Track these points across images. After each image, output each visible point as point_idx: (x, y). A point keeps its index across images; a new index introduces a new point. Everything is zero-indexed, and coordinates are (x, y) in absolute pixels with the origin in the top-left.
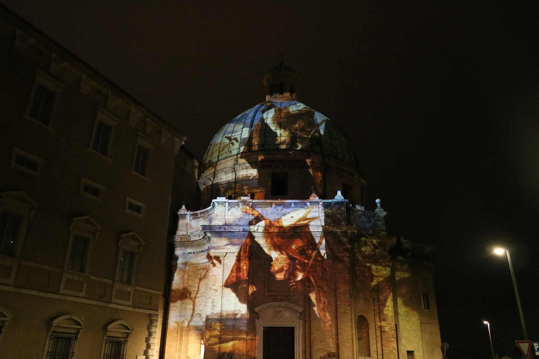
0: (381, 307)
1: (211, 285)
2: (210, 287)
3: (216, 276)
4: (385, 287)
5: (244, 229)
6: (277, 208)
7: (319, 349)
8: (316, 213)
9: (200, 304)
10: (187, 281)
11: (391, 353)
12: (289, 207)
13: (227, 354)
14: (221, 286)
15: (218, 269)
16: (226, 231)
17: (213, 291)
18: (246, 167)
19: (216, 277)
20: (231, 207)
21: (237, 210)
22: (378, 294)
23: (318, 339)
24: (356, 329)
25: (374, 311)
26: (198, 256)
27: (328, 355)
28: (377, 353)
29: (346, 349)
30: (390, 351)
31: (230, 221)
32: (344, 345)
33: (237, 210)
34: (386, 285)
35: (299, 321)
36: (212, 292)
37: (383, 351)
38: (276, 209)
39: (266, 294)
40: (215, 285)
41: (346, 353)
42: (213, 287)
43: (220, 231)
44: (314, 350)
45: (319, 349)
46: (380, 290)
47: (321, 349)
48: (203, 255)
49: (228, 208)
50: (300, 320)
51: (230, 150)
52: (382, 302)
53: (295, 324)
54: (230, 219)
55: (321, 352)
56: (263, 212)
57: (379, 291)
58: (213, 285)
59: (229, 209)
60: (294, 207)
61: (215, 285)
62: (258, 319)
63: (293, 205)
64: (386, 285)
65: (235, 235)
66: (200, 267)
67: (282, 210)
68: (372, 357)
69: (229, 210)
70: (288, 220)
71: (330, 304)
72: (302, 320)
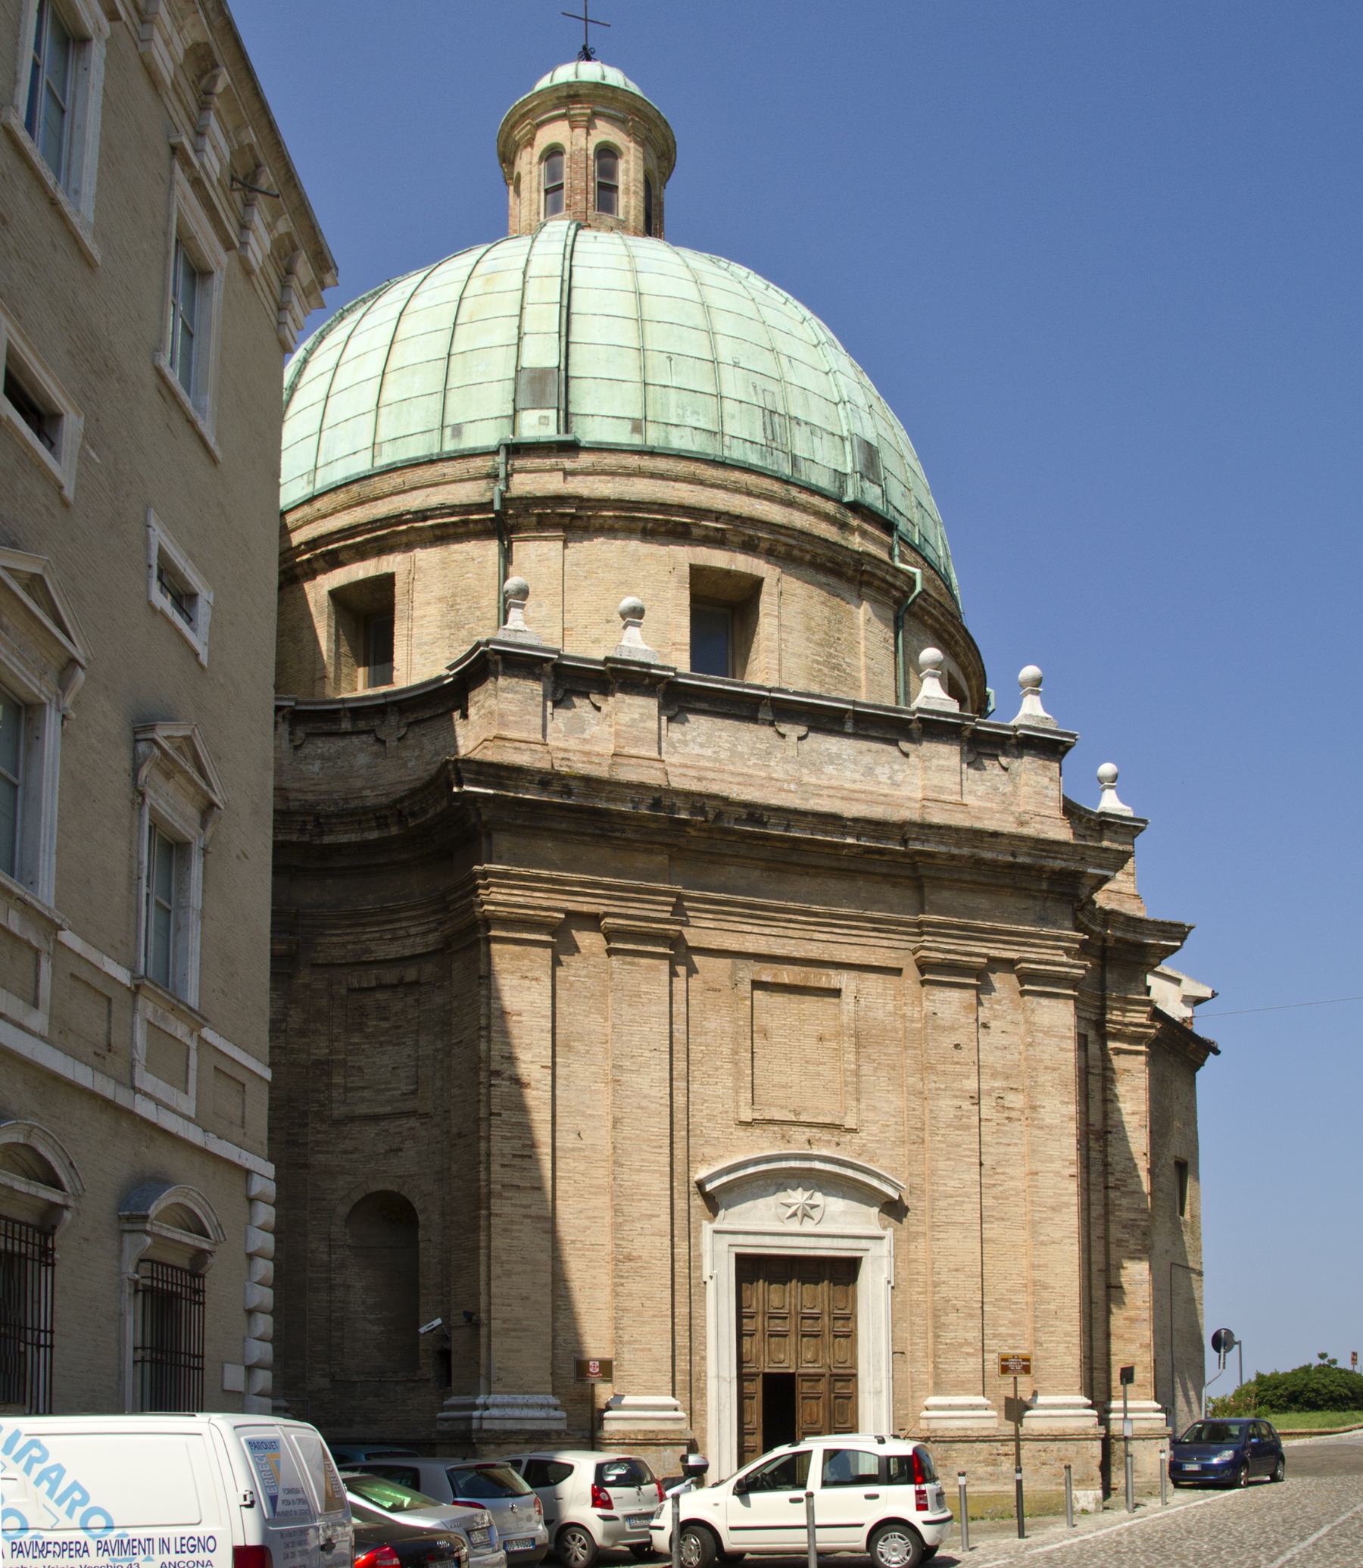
1: (498, 1058)
2: (495, 1066)
3: (519, 1015)
6: (781, 730)
7: (961, 1345)
8: (946, 776)
9: (391, 1150)
13: (597, 1363)
15: (527, 983)
17: (506, 1086)
19: (520, 1022)
21: (598, 709)
22: (1106, 1146)
26: (364, 925)
27: (1003, 1366)
29: (1058, 1342)
31: (568, 759)
32: (1051, 1329)
36: (507, 1090)
39: (747, 1115)
41: (1056, 1357)
45: (961, 1345)
48: (399, 920)
50: (885, 1228)
51: (451, 420)
53: (864, 1244)
54: (566, 750)
56: (720, 737)
63: (849, 728)
65: (607, 826)
66: (377, 979)
67: (800, 739)
70: (832, 792)
71: (999, 1170)
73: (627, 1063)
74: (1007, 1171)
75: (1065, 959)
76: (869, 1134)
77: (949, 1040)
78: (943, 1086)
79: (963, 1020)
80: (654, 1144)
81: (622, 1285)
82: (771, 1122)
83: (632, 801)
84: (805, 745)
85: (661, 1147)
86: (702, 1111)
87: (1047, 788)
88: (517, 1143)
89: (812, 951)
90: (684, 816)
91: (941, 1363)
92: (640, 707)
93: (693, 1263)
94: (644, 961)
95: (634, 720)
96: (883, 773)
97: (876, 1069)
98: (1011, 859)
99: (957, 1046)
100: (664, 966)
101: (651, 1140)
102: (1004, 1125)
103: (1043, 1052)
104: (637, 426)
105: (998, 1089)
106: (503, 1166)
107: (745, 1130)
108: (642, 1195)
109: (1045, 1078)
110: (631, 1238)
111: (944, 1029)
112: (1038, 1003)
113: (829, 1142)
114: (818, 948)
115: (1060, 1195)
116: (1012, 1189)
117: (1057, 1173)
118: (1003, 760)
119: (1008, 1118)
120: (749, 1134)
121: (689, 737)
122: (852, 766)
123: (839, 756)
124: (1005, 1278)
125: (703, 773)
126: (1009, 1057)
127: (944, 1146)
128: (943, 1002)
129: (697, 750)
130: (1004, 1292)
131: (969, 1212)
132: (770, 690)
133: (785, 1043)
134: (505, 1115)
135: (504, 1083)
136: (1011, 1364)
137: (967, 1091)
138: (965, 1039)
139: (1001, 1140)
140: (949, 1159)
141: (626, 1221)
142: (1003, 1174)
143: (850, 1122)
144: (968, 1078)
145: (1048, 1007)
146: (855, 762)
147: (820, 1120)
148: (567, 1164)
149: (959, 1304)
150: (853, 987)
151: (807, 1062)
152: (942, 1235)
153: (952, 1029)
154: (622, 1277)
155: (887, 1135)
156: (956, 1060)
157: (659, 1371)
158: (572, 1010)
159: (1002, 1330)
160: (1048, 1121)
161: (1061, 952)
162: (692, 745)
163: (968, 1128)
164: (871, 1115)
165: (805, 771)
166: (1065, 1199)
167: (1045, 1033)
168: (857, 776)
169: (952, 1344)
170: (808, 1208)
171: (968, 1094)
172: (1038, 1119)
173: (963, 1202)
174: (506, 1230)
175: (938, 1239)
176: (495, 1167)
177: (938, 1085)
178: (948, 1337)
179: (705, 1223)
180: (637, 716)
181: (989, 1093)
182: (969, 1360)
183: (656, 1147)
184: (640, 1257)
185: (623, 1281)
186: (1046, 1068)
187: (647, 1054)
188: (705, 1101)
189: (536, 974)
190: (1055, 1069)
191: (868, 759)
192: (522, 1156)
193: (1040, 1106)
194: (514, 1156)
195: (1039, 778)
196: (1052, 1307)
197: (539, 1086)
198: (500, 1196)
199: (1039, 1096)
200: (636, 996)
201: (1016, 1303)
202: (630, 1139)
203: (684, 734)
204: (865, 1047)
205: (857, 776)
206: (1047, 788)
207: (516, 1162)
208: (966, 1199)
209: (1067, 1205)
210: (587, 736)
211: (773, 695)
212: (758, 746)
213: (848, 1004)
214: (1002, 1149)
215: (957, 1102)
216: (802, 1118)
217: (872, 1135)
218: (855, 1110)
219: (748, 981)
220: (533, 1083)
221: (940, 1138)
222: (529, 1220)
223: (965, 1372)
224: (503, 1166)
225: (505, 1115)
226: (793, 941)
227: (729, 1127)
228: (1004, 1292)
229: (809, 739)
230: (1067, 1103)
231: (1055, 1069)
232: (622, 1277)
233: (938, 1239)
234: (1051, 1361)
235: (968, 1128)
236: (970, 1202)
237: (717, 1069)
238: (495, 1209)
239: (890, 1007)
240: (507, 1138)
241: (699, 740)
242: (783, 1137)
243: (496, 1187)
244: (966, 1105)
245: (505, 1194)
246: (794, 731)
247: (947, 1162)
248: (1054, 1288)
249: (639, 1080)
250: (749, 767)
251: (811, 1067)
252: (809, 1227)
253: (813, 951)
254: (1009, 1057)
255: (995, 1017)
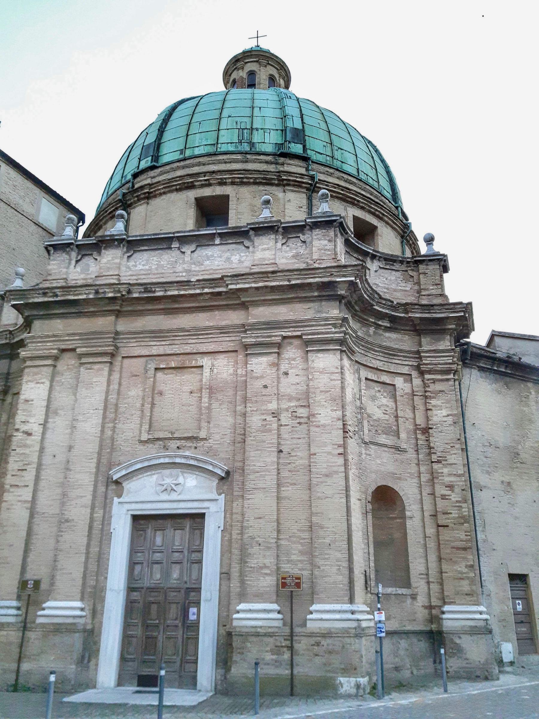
0: (435, 466)
2: (17, 427)
3: (32, 401)
4: (445, 419)
5: (97, 292)
6: (183, 250)
7: (261, 568)
10: (5, 427)
11: (462, 579)
12: (208, 245)
14: (41, 424)
15: (38, 385)
16: (59, 299)
17: (21, 436)
18: (145, 193)
19: (31, 404)
20: (84, 256)
21: (96, 259)
23: (260, 542)
24: (370, 516)
25: (419, 477)
27: (282, 582)
28: (428, 578)
30: (462, 573)
32: (326, 556)
33: (96, 259)
34: (448, 416)
35: (217, 497)
36: (21, 438)
37: (443, 574)
38: (181, 252)
39: (145, 437)
40: (28, 422)
41: (330, 576)
42: (22, 426)
43: (46, 299)
44: (250, 569)
45: (261, 568)
46: (432, 428)
47: (266, 567)
49: (77, 258)
50: (220, 494)
52: (439, 454)
53: (206, 504)
55: (266, 574)
56: (153, 260)
57: (430, 430)
58: (24, 422)
59: (79, 258)
60: (221, 244)
61: (28, 422)
62: (119, 496)
64: (448, 416)
68: (416, 588)
69: (77, 261)
71: (292, 454)
72: (223, 495)
73: (80, 418)
74: (298, 454)
75: (333, 330)
76: (214, 441)
77: (259, 384)
78: (255, 409)
79: (268, 372)
80: (90, 457)
81: (62, 536)
82: (158, 439)
83: (86, 294)
84: (195, 255)
85: (92, 459)
86: (122, 438)
87: (326, 245)
88: (21, 464)
89: (187, 349)
90: (111, 295)
91: (247, 580)
92: (112, 254)
93: (106, 520)
94: (96, 367)
95: (109, 260)
96: (235, 258)
97: (220, 404)
98: (288, 283)
99: (265, 387)
100: (106, 368)
101: (87, 456)
102: (296, 427)
103: (319, 382)
104: (182, 152)
105: (293, 407)
106: (13, 475)
107: (144, 445)
108: (79, 485)
109: (320, 397)
110: (70, 509)
111: (257, 378)
112: (316, 356)
113: (190, 447)
114: (191, 347)
115: (331, 466)
116: (302, 465)
117: (329, 453)
118: (302, 237)
119: (299, 423)
120: (145, 447)
121: (138, 263)
122: (219, 259)
123: (212, 256)
124: (296, 522)
125: (140, 277)
126: (301, 388)
127: (254, 442)
128: (256, 364)
129: (141, 267)
130: (296, 531)
131: (270, 481)
132: (174, 233)
133: (172, 397)
134: (18, 450)
135: (20, 434)
136: (288, 581)
137: (271, 410)
138: (270, 382)
139: (294, 436)
140: (257, 450)
141: (68, 500)
142: (295, 456)
143: (202, 435)
144: (271, 402)
145: (321, 357)
146: (221, 257)
147: (186, 435)
148: (46, 472)
149: (260, 540)
150: (210, 363)
151: (183, 405)
152: (250, 497)
153: (262, 377)
154: (62, 531)
155: (225, 440)
156: (263, 393)
157: (75, 586)
158: (60, 395)
159: (294, 557)
160: (323, 422)
161: (330, 327)
162: (139, 266)
163: (270, 431)
164: (216, 430)
165: (193, 266)
166: (335, 469)
167: (321, 372)
168: (220, 263)
169: (254, 568)
170: (173, 486)
171: (271, 412)
172: (316, 421)
173: (266, 475)
174: (8, 509)
175: (249, 499)
176: (9, 476)
177: (252, 409)
178: (253, 562)
179: (115, 499)
180: (110, 259)
181: (287, 410)
182: (267, 578)
183: (90, 459)
184: (73, 520)
185: (62, 534)
186: (321, 392)
187: (92, 411)
188: (125, 432)
189: (43, 381)
190: (328, 392)
191: (228, 254)
192: (23, 470)
193: (317, 414)
194: (19, 470)
195: (322, 242)
196: (327, 541)
197: (36, 434)
198: (9, 491)
199: (317, 408)
200: (90, 384)
201: (304, 539)
202: (77, 456)
203: (135, 262)
204: (215, 394)
205: (223, 263)
206: (326, 245)
207: (19, 473)
208: (267, 473)
209: (336, 472)
210: (90, 272)
211: (175, 235)
212: (172, 259)
213: (206, 373)
214: (295, 441)
215: (264, 417)
216: (175, 436)
217: (216, 441)
218: (206, 428)
219: (153, 369)
220: (33, 434)
221: (252, 438)
222: (20, 503)
223: (264, 587)
224: (13, 475)
225: (18, 450)
226: (177, 346)
227: (136, 444)
228: (296, 531)
229: (197, 252)
230: (336, 410)
231: (328, 392)
232: (62, 531)
233: (249, 499)
234: (327, 579)
235: (270, 431)
236: (270, 475)
237: (132, 415)
238: (5, 499)
239: (231, 371)
240: (17, 461)
241: (143, 263)
242: (164, 447)
243: (7, 487)
244: (269, 418)
245: (11, 490)
246: (188, 249)
247: (256, 452)
248: (328, 528)
249: (85, 425)
250: (165, 270)
251: (184, 408)
252: (174, 496)
253: (188, 349)
254: (301, 388)
255: (292, 368)
